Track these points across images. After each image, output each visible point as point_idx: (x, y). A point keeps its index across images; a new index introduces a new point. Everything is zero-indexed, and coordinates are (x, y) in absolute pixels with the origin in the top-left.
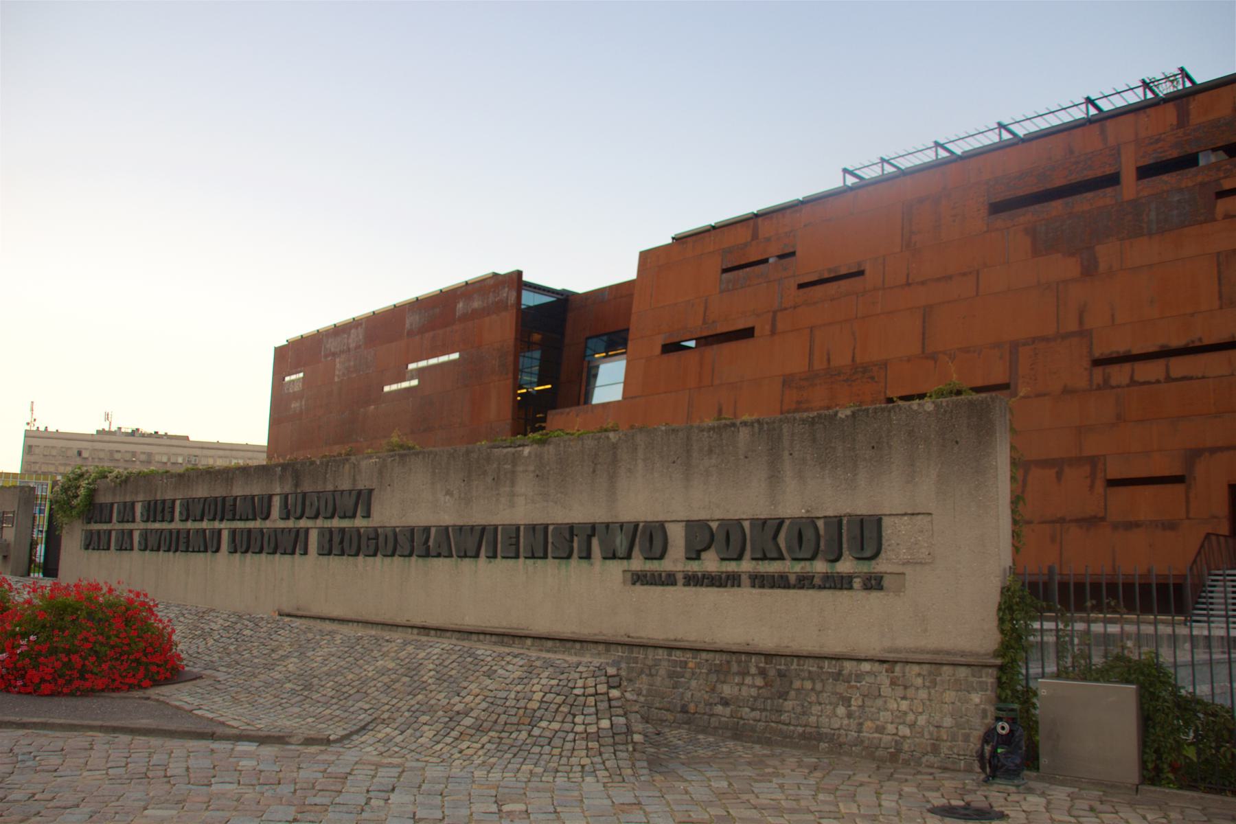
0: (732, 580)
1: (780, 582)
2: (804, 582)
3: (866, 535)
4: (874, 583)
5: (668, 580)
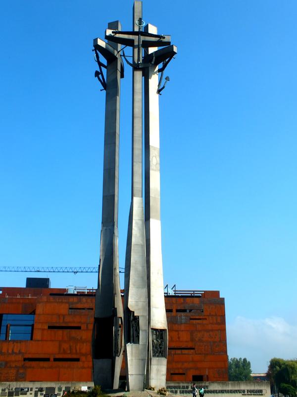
0: (251, 395)
1: (255, 395)
2: (257, 395)
3: (261, 391)
4: (262, 395)
5: (246, 395)
